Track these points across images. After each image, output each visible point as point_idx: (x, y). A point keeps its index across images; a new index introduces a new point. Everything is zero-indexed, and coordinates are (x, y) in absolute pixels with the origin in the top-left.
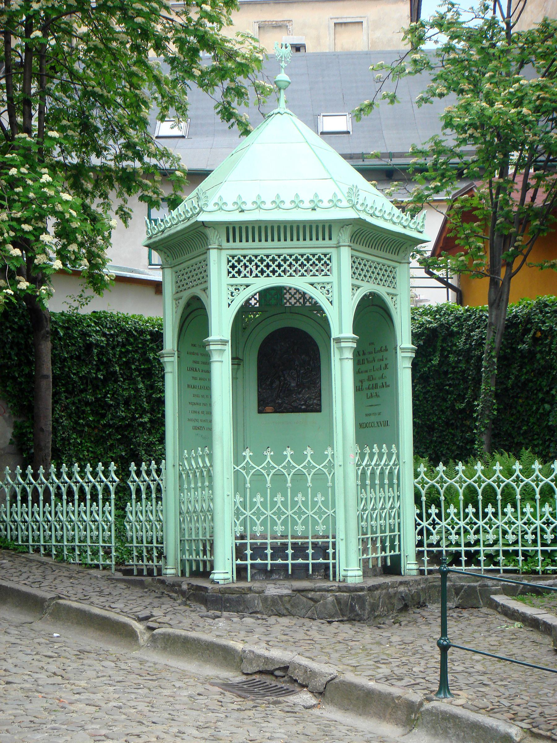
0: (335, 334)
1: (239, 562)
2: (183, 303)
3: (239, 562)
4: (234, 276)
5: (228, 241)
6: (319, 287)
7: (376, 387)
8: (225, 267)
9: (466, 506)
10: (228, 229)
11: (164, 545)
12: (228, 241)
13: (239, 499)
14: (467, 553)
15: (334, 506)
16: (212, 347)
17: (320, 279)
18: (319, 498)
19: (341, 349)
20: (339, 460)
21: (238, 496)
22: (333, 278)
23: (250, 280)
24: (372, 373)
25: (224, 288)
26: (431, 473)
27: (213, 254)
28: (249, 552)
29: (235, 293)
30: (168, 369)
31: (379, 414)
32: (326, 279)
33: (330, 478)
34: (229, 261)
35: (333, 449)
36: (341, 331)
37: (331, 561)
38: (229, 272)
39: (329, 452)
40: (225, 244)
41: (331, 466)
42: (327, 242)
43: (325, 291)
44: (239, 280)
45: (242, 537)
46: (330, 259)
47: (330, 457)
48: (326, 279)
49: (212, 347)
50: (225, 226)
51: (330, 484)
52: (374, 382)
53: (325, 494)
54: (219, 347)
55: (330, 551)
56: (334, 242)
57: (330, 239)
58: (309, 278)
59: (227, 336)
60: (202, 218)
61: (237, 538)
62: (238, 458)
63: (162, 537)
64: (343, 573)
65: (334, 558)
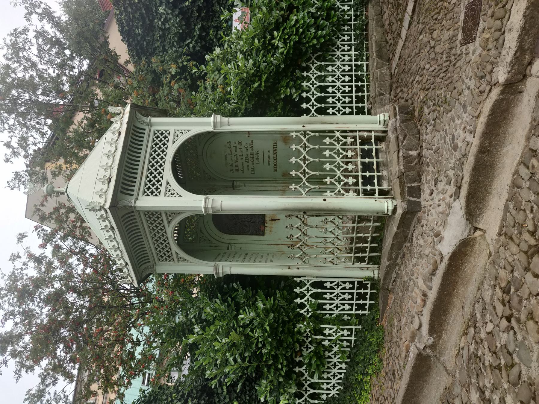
0: (210, 129)
1: (377, 195)
2: (182, 254)
3: (377, 195)
4: (159, 193)
5: (132, 195)
6: (176, 138)
7: (252, 154)
8: (151, 198)
9: (328, 92)
10: (121, 192)
11: (356, 280)
12: (132, 195)
13: (328, 193)
14: (357, 92)
15: (332, 132)
16: (210, 206)
17: (171, 138)
18: (327, 140)
19: (222, 124)
20: (300, 127)
21: (325, 194)
22: (172, 129)
23: (164, 182)
24: (244, 157)
25: (166, 198)
26: (307, 112)
27: (139, 204)
28: (369, 188)
29: (172, 192)
30: (227, 271)
31: (269, 151)
32: (172, 134)
33: (312, 134)
34: (148, 195)
35: (292, 132)
36: (208, 124)
37: (373, 134)
38: (156, 195)
39: (294, 135)
40: (135, 197)
41: (305, 133)
42: (146, 132)
43: (180, 135)
44: (163, 189)
45: (357, 192)
46: (158, 131)
47: (298, 134)
48: (172, 134)
49: (210, 206)
50: (119, 194)
51: (317, 134)
52: (249, 156)
53: (325, 137)
54: (210, 201)
55: (365, 134)
56: (147, 128)
57: (145, 130)
58: (169, 144)
59: (203, 197)
60: (107, 206)
61: (358, 195)
62: (297, 193)
63: (351, 283)
64: (381, 126)
65: (370, 131)
